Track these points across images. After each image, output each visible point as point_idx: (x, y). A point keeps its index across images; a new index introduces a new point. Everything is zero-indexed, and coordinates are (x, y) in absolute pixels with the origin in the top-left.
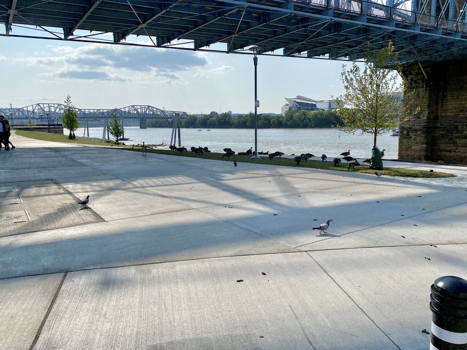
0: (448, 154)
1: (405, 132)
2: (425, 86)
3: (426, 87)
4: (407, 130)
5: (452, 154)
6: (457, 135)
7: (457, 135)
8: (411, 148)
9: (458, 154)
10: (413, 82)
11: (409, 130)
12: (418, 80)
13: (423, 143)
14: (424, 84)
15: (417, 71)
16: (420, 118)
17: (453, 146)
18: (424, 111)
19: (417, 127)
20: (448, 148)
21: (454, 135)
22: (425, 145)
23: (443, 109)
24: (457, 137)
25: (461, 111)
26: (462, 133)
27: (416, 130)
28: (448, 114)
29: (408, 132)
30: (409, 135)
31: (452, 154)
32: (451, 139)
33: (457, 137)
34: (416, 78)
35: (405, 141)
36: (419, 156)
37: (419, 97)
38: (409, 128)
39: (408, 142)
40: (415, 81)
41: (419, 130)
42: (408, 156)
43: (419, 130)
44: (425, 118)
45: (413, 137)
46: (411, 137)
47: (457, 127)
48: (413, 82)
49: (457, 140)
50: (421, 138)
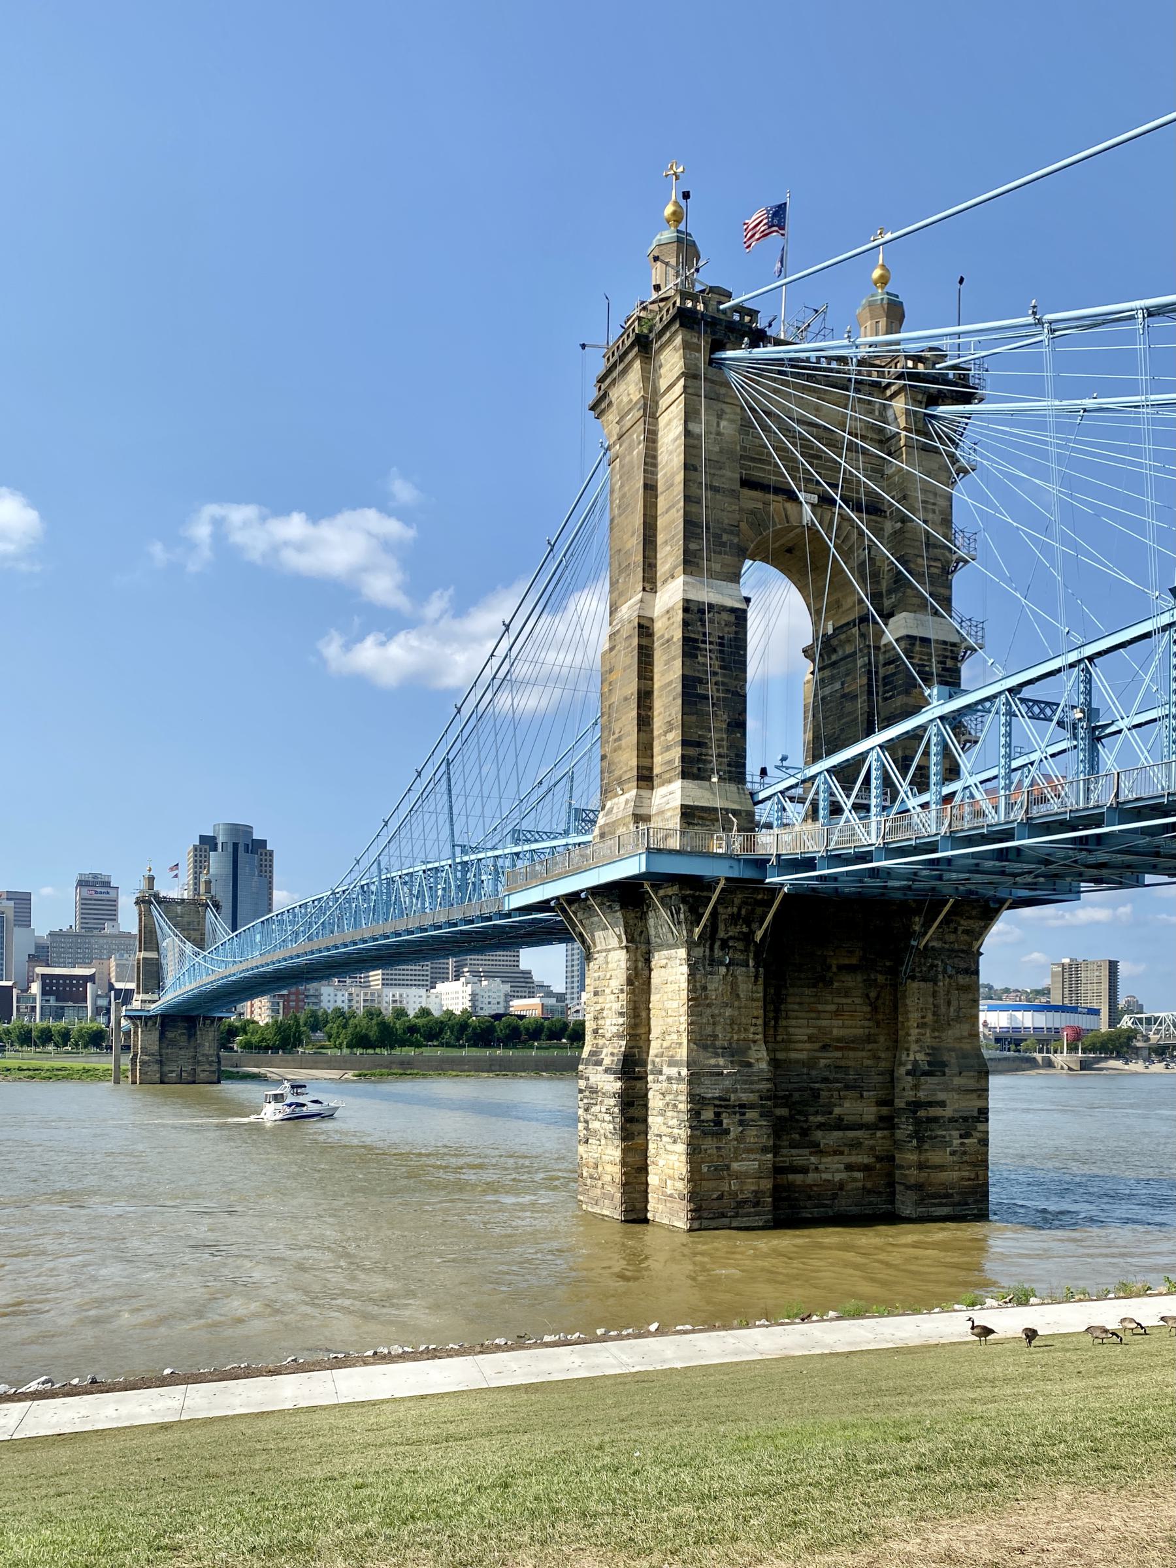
0: (798, 1178)
1: (708, 1114)
2: (751, 963)
3: (757, 966)
4: (716, 1106)
5: (811, 1177)
6: (820, 1119)
7: (820, 1119)
8: (728, 1167)
9: (824, 1176)
10: (717, 945)
11: (723, 1104)
12: (731, 938)
13: (764, 1150)
14: (751, 955)
15: (735, 910)
16: (749, 1065)
17: (811, 1154)
18: (755, 1042)
19: (745, 1097)
20: (799, 1161)
21: (811, 1118)
22: (770, 1156)
23: (779, 1038)
24: (821, 1126)
25: (825, 1048)
26: (831, 1113)
27: (742, 1106)
28: (794, 1055)
29: (717, 1114)
30: (720, 1123)
31: (811, 1177)
32: (805, 1133)
33: (821, 1126)
34: (727, 931)
35: (709, 1144)
36: (755, 1192)
37: (738, 995)
38: (720, 1099)
39: (719, 1148)
40: (724, 945)
41: (752, 1106)
42: (720, 1198)
43: (752, 1106)
44: (763, 1066)
45: (735, 1131)
46: (727, 1132)
47: (816, 1094)
48: (717, 945)
49: (819, 1135)
50: (758, 1134)
